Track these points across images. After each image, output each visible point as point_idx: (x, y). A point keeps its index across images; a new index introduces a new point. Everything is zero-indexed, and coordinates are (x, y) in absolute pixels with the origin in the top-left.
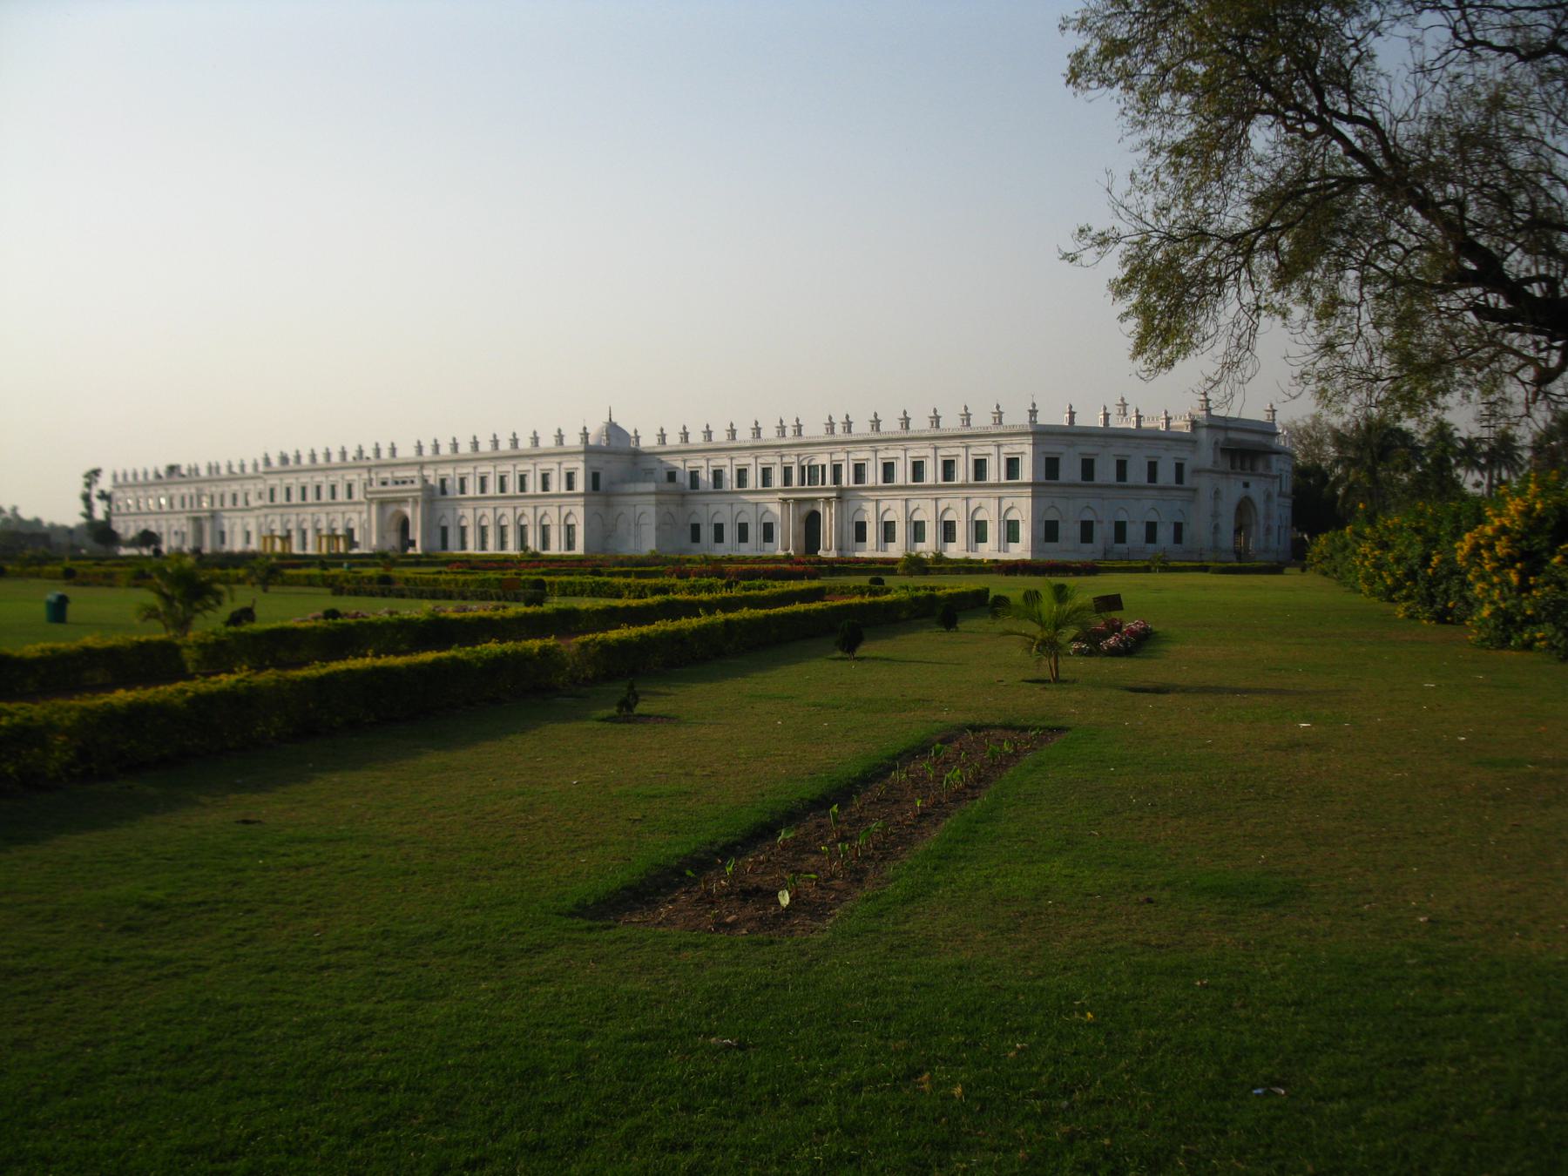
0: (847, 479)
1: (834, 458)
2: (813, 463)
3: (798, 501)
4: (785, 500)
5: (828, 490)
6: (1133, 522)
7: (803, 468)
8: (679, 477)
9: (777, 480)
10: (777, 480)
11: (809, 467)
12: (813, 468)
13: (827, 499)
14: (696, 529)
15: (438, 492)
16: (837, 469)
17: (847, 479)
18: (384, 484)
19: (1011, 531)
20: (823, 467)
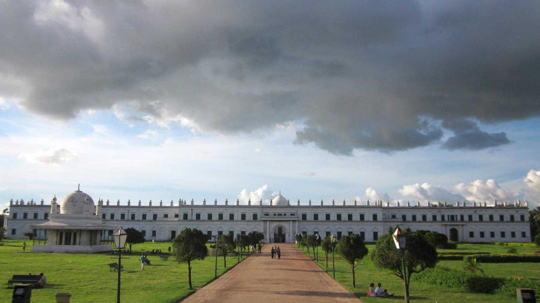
0: (466, 218)
1: (461, 213)
2: (452, 214)
3: (450, 225)
4: (446, 225)
5: (460, 222)
7: (448, 216)
9: (439, 218)
10: (439, 218)
12: (452, 217)
13: (462, 225)
15: (301, 218)
16: (462, 217)
17: (466, 218)
18: (275, 215)
20: (456, 216)
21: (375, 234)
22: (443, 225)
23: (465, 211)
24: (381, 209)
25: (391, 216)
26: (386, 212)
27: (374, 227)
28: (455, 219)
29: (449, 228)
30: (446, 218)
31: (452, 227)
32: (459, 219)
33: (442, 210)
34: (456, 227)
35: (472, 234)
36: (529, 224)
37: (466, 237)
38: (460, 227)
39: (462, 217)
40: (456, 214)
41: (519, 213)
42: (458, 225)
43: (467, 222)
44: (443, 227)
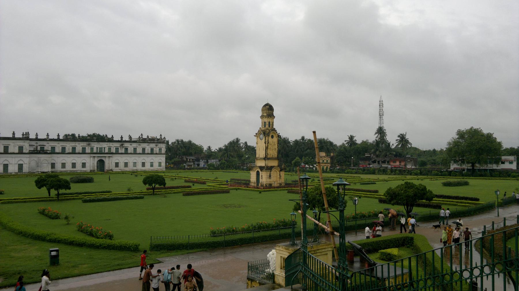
1: (109, 145)
2: (100, 147)
4: (94, 157)
5: (107, 153)
6: (147, 162)
7: (97, 148)
8: (46, 148)
9: (88, 150)
11: (99, 148)
12: (101, 148)
13: (109, 157)
14: (53, 165)
16: (110, 149)
17: (113, 150)
19: (160, 165)
20: (104, 148)
21: (21, 167)
22: (91, 156)
23: (113, 144)
24: (28, 141)
25: (39, 148)
26: (33, 143)
27: (20, 159)
28: (103, 152)
29: (96, 160)
30: (95, 151)
31: (99, 159)
32: (107, 151)
33: (91, 143)
34: (103, 159)
35: (117, 165)
36: (165, 156)
37: (113, 167)
38: (107, 158)
39: (110, 149)
40: (105, 147)
41: (158, 146)
42: (105, 157)
43: (112, 153)
44: (92, 158)
